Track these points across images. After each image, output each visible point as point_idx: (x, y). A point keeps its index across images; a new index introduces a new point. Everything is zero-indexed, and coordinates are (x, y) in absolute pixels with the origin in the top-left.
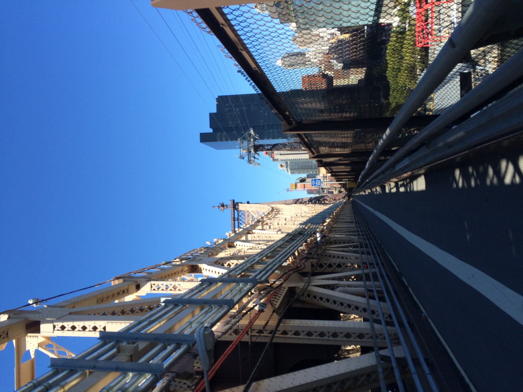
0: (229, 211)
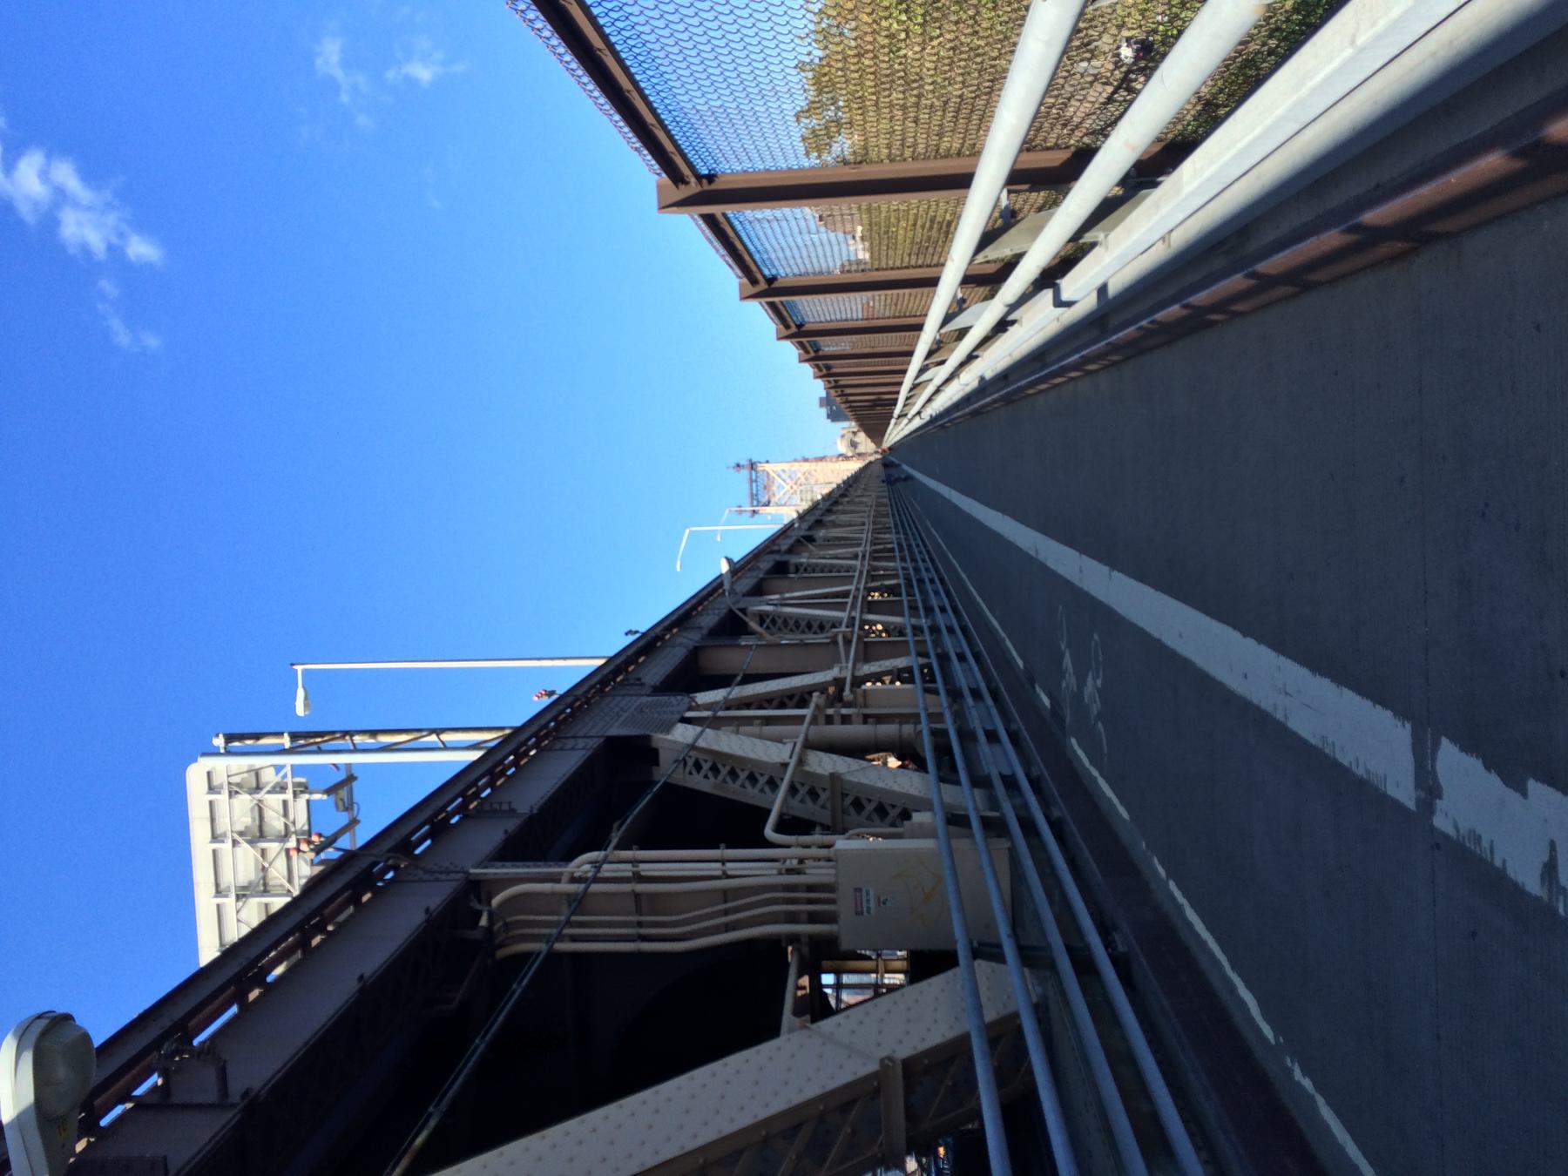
0: (745, 473)
